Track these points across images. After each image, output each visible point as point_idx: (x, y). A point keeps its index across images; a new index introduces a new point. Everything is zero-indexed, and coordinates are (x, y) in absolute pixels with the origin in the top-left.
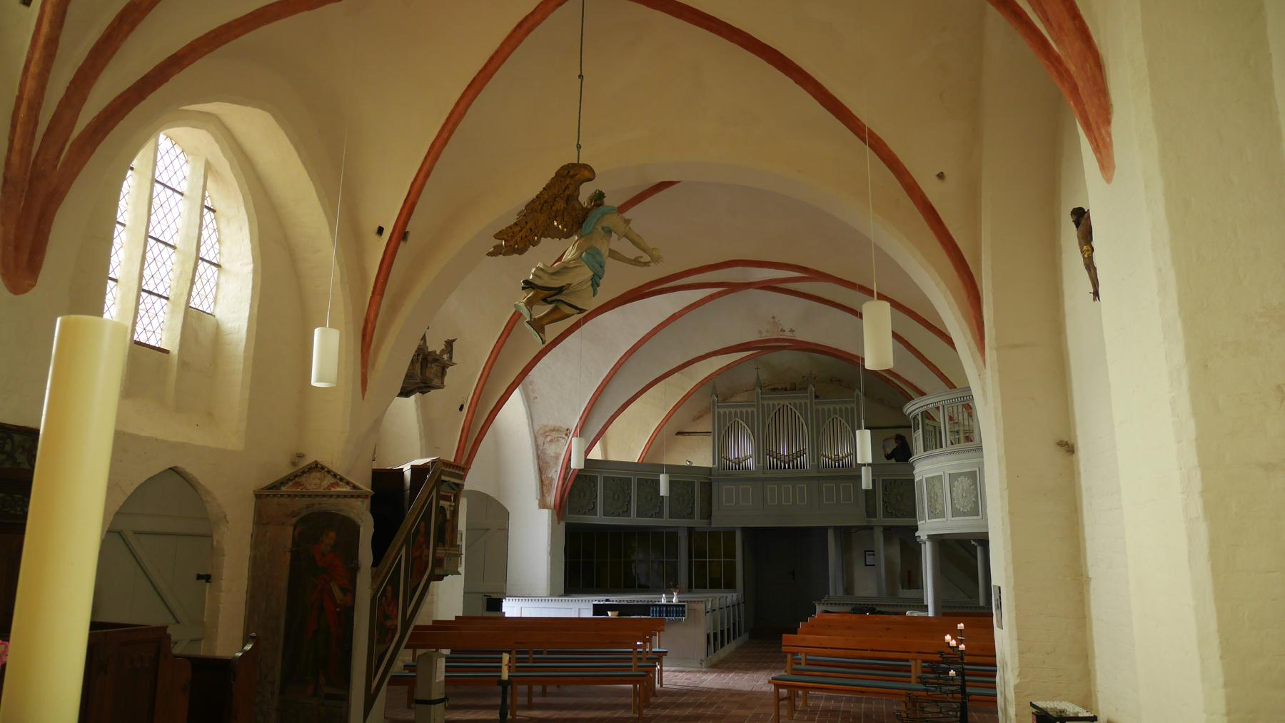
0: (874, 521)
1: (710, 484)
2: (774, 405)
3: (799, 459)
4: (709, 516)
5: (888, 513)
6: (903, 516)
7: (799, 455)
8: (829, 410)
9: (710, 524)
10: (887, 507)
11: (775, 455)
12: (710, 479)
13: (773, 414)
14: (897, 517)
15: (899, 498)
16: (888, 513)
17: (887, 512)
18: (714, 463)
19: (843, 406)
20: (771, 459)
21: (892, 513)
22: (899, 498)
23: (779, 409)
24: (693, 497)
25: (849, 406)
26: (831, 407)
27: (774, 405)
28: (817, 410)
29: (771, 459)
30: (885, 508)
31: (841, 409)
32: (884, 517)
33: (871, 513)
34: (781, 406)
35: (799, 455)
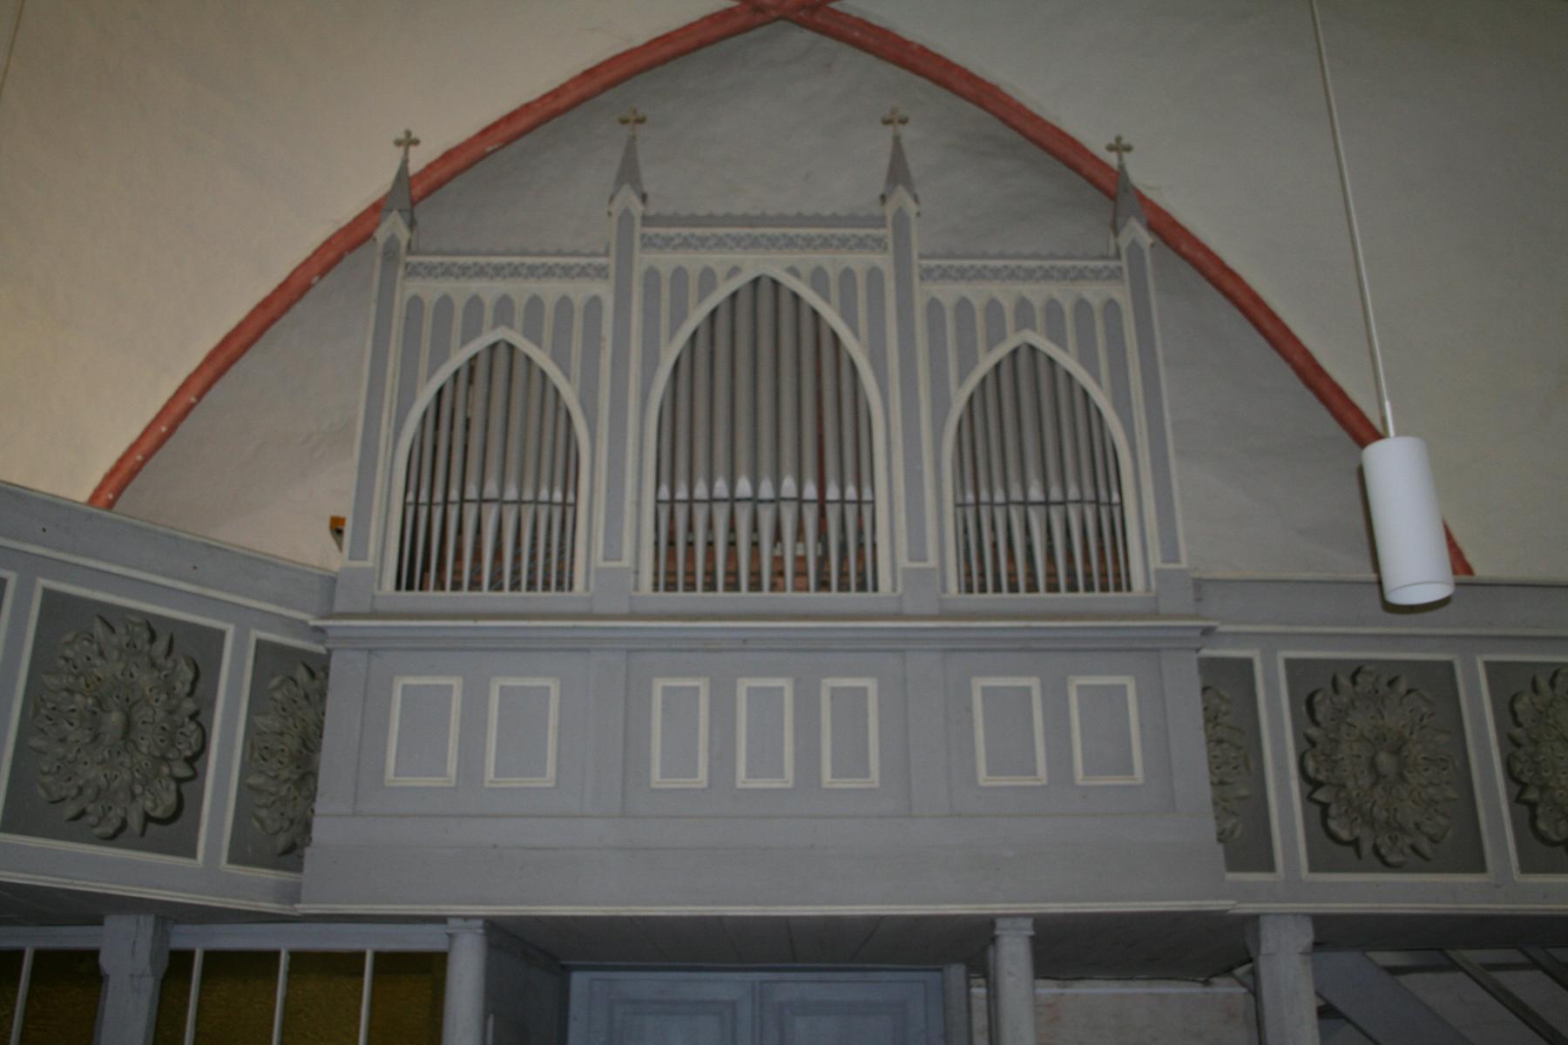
15: (1384, 759)
17: (1333, 837)
21: (1355, 843)
22: (1384, 759)
30: (1321, 815)
32: (1314, 867)
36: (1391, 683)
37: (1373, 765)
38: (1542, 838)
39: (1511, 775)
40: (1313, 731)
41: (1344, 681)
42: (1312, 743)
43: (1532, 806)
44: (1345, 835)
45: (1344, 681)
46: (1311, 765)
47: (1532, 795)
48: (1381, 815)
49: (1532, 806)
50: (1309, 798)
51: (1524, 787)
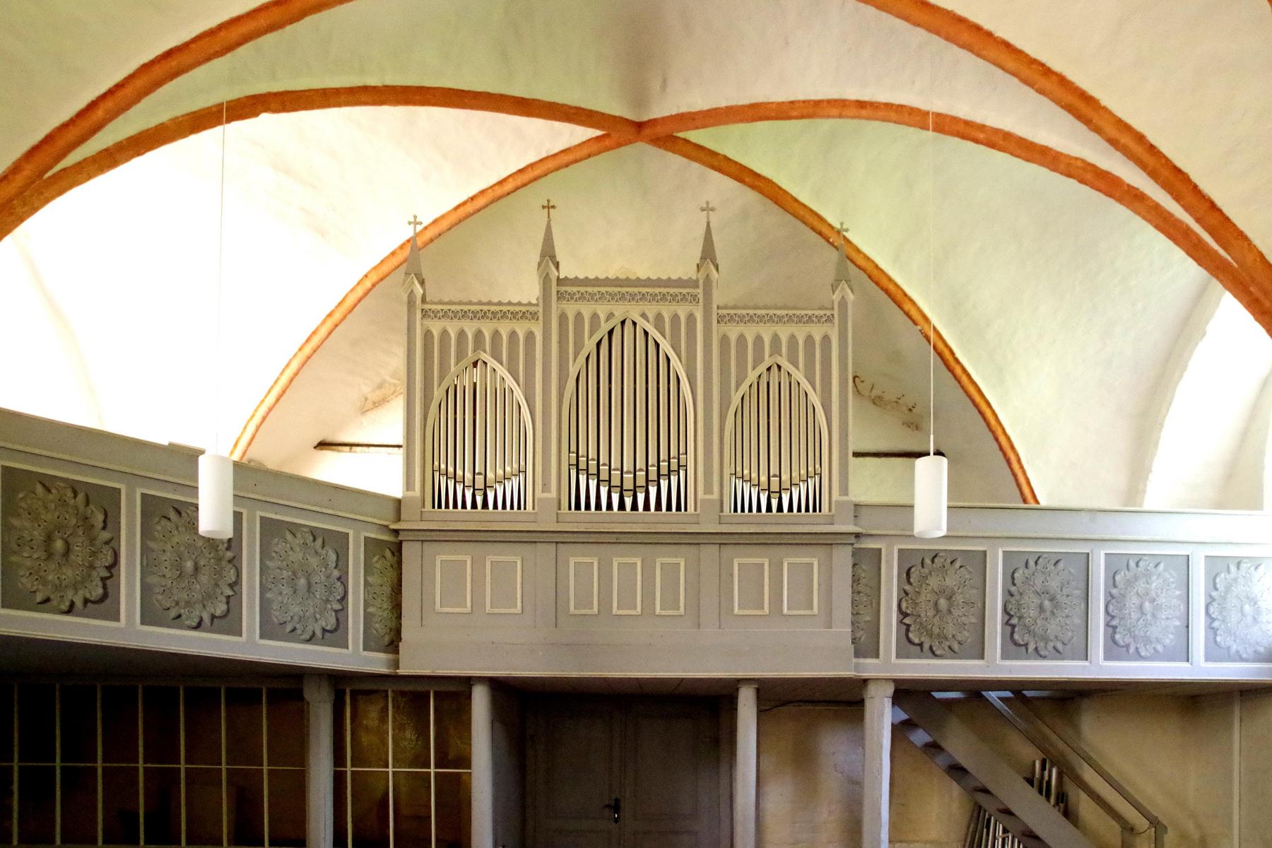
0: (869, 668)
1: (397, 549)
2: (595, 317)
3: (664, 484)
4: (393, 645)
5: (909, 645)
6: (953, 653)
7: (664, 471)
8: (759, 340)
9: (396, 664)
10: (908, 626)
11: (593, 470)
12: (396, 532)
13: (590, 345)
14: (935, 655)
15: (943, 603)
16: (909, 645)
17: (910, 641)
18: (409, 485)
19: (801, 333)
20: (583, 478)
21: (921, 645)
23: (611, 333)
24: (343, 580)
25: (817, 332)
26: (766, 333)
27: (595, 317)
28: (724, 340)
29: (583, 478)
31: (793, 340)
33: (866, 645)
34: (616, 321)
35: (664, 471)
36: (952, 562)
37: (936, 604)
38: (1016, 644)
39: (1005, 611)
40: (907, 587)
41: (928, 561)
42: (906, 593)
43: (1013, 627)
44: (916, 641)
45: (928, 561)
46: (904, 605)
47: (1014, 621)
48: (936, 630)
49: (1013, 627)
50: (901, 622)
51: (1011, 616)
